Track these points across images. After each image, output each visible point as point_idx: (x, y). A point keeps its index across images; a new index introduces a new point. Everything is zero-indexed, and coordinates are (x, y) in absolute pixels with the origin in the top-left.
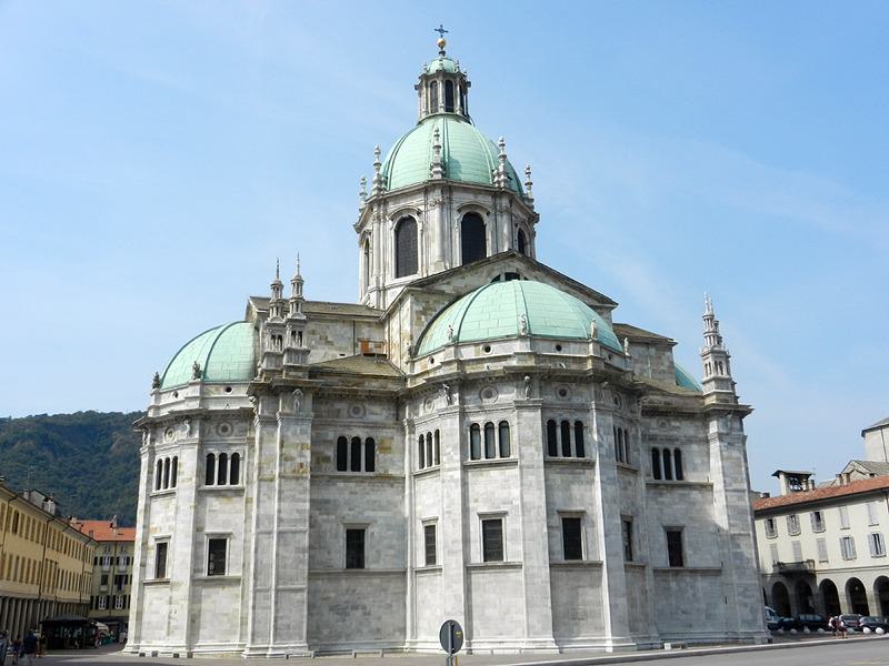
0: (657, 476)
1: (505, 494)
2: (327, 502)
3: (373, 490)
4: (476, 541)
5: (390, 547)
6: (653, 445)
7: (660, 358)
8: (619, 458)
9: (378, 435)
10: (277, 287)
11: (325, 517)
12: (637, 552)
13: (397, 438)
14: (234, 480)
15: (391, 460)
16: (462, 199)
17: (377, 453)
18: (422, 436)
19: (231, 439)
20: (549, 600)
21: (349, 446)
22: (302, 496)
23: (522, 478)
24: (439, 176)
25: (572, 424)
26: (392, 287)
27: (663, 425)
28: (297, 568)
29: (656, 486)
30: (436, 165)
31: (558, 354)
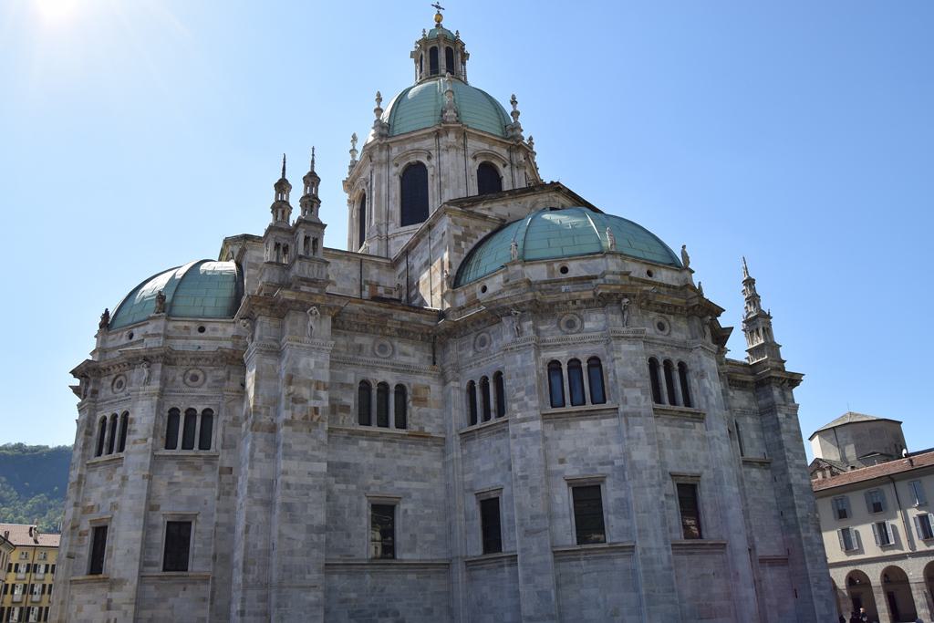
1: (600, 451)
2: (346, 465)
3: (405, 453)
4: (564, 516)
5: (429, 530)
9: (412, 381)
11: (343, 486)
13: (435, 388)
14: (205, 445)
15: (428, 415)
16: (474, 145)
17: (410, 404)
18: (472, 383)
19: (203, 391)
21: (374, 393)
22: (316, 453)
26: (396, 235)
28: (308, 554)
31: (650, 279)
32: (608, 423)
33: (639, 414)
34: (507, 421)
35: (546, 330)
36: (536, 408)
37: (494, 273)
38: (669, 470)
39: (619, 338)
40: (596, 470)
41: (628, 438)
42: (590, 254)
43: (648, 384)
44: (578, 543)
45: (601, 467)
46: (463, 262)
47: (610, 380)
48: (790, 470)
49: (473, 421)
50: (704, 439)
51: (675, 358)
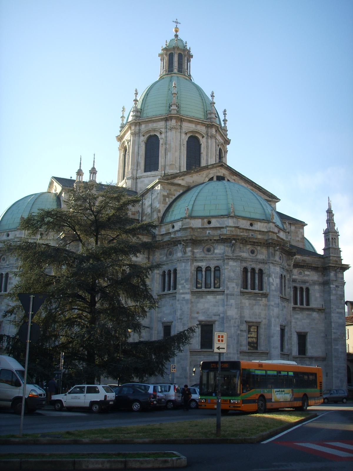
0: (296, 303)
6: (294, 285)
7: (297, 233)
8: (281, 293)
10: (80, 173)
12: (286, 347)
16: (187, 126)
18: (164, 272)
25: (257, 271)
27: (300, 273)
30: (174, 104)
31: (251, 228)
32: (219, 297)
33: (232, 295)
34: (176, 293)
35: (197, 252)
36: (188, 289)
37: (178, 221)
38: (245, 319)
39: (229, 259)
40: (211, 317)
41: (227, 305)
42: (222, 215)
43: (240, 282)
44: (201, 348)
45: (214, 317)
46: (166, 209)
47: (223, 278)
48: (332, 315)
49: (164, 290)
50: (266, 305)
51: (257, 267)
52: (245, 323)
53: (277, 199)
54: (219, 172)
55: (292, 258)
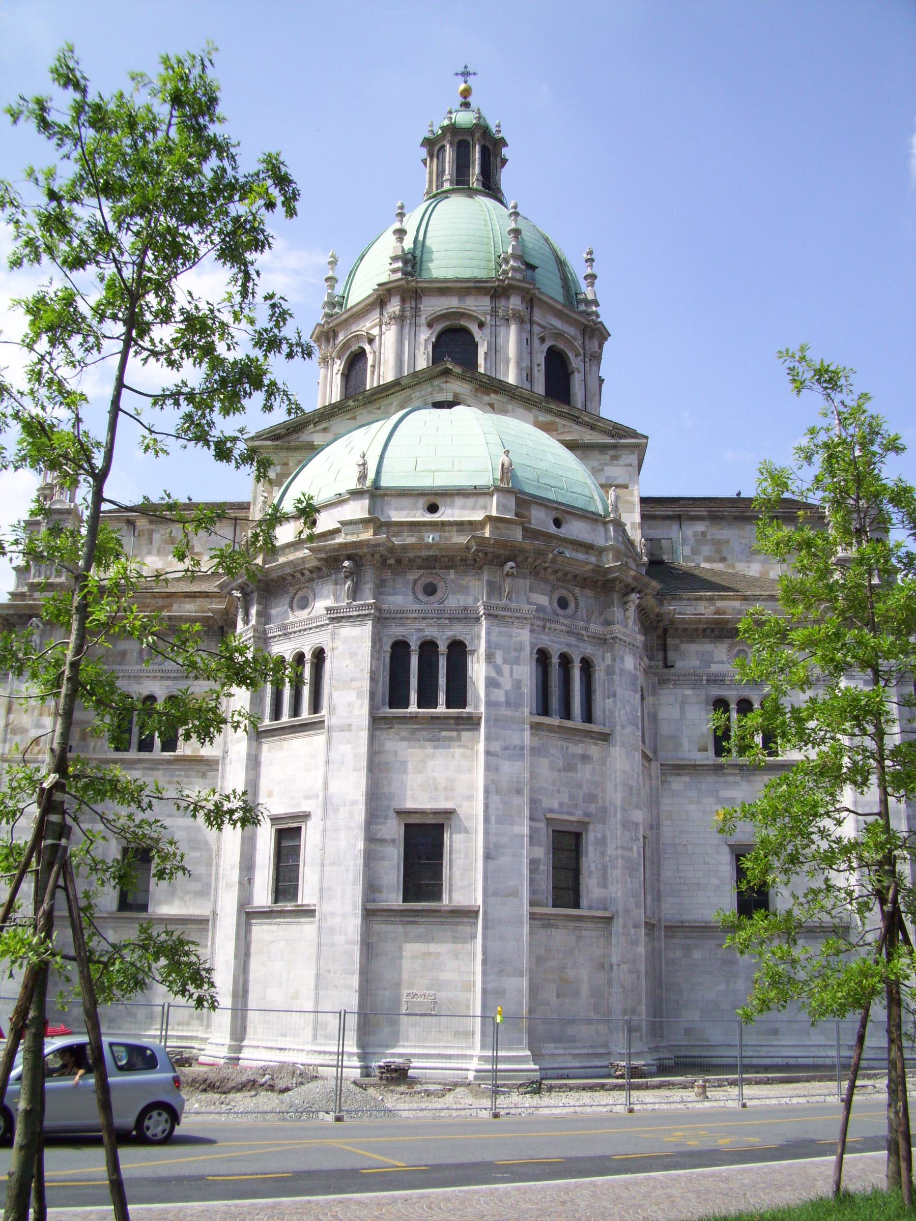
16: (432, 306)
20: (356, 977)
23: (328, 750)
24: (399, 275)
25: (443, 648)
29: (718, 768)
30: (395, 259)
33: (348, 728)
44: (276, 901)
52: (395, 815)
53: (633, 437)
54: (441, 390)
55: (625, 599)
